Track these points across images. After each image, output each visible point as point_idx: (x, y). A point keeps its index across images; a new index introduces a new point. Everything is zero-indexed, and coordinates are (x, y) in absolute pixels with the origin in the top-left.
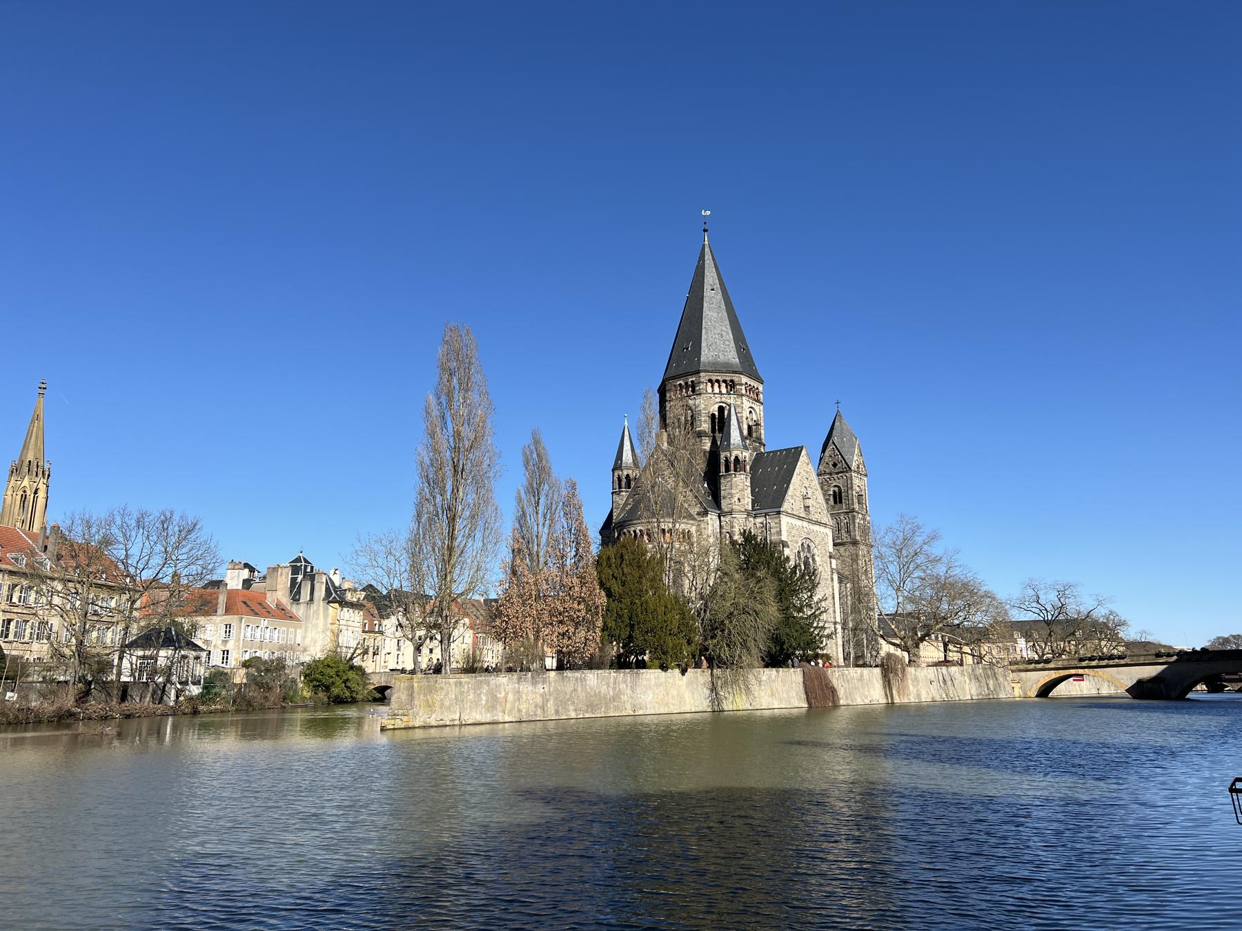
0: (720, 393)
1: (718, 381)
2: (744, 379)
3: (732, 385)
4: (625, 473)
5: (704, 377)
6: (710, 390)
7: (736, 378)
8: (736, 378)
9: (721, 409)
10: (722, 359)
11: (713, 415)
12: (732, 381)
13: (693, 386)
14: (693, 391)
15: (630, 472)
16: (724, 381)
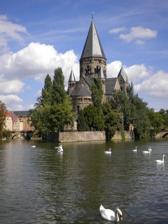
0: (97, 63)
1: (97, 60)
2: (103, 59)
3: (100, 61)
4: (72, 82)
5: (93, 59)
6: (94, 62)
7: (101, 59)
8: (101, 59)
9: (97, 67)
10: (98, 54)
11: (95, 68)
12: (100, 60)
13: (90, 61)
14: (90, 62)
15: (73, 82)
16: (98, 60)
